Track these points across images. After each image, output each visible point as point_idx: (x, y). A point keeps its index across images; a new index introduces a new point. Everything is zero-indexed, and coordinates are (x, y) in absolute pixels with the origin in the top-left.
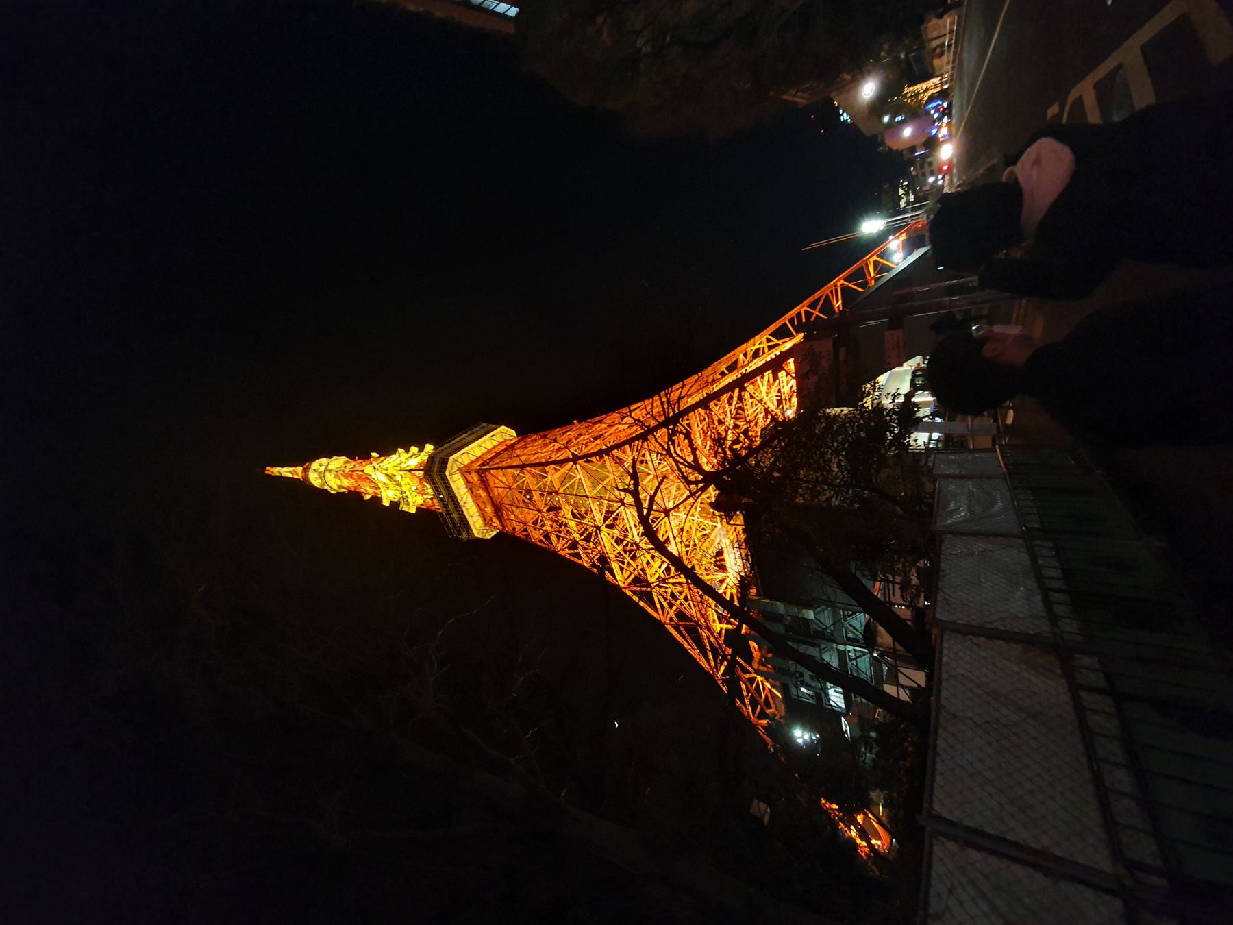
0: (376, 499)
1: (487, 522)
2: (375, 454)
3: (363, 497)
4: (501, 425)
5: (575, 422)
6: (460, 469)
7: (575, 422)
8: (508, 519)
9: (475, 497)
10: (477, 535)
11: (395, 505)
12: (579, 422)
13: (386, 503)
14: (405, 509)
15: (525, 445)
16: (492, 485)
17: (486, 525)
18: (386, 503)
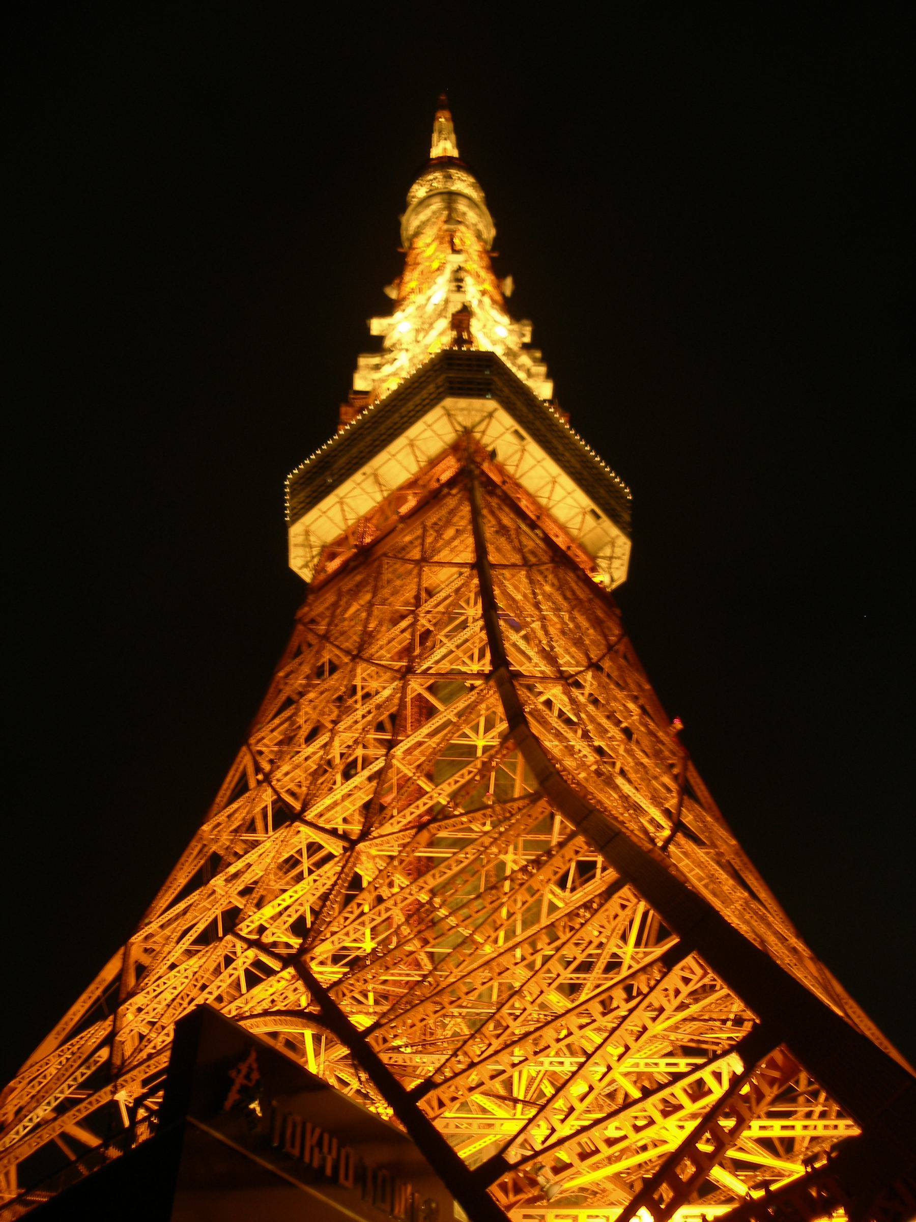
0: (388, 308)
1: (329, 552)
2: (508, 285)
3: (389, 282)
4: (632, 536)
5: (678, 725)
6: (467, 432)
7: (678, 725)
8: (340, 595)
9: (396, 498)
10: (296, 532)
11: (376, 346)
12: (680, 736)
13: (377, 326)
14: (363, 361)
15: (580, 601)
16: (432, 517)
17: (324, 547)
18: (377, 326)
